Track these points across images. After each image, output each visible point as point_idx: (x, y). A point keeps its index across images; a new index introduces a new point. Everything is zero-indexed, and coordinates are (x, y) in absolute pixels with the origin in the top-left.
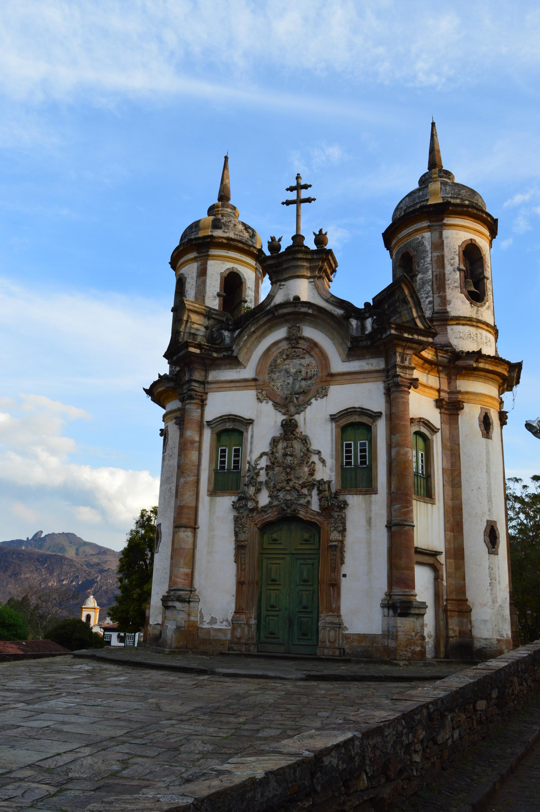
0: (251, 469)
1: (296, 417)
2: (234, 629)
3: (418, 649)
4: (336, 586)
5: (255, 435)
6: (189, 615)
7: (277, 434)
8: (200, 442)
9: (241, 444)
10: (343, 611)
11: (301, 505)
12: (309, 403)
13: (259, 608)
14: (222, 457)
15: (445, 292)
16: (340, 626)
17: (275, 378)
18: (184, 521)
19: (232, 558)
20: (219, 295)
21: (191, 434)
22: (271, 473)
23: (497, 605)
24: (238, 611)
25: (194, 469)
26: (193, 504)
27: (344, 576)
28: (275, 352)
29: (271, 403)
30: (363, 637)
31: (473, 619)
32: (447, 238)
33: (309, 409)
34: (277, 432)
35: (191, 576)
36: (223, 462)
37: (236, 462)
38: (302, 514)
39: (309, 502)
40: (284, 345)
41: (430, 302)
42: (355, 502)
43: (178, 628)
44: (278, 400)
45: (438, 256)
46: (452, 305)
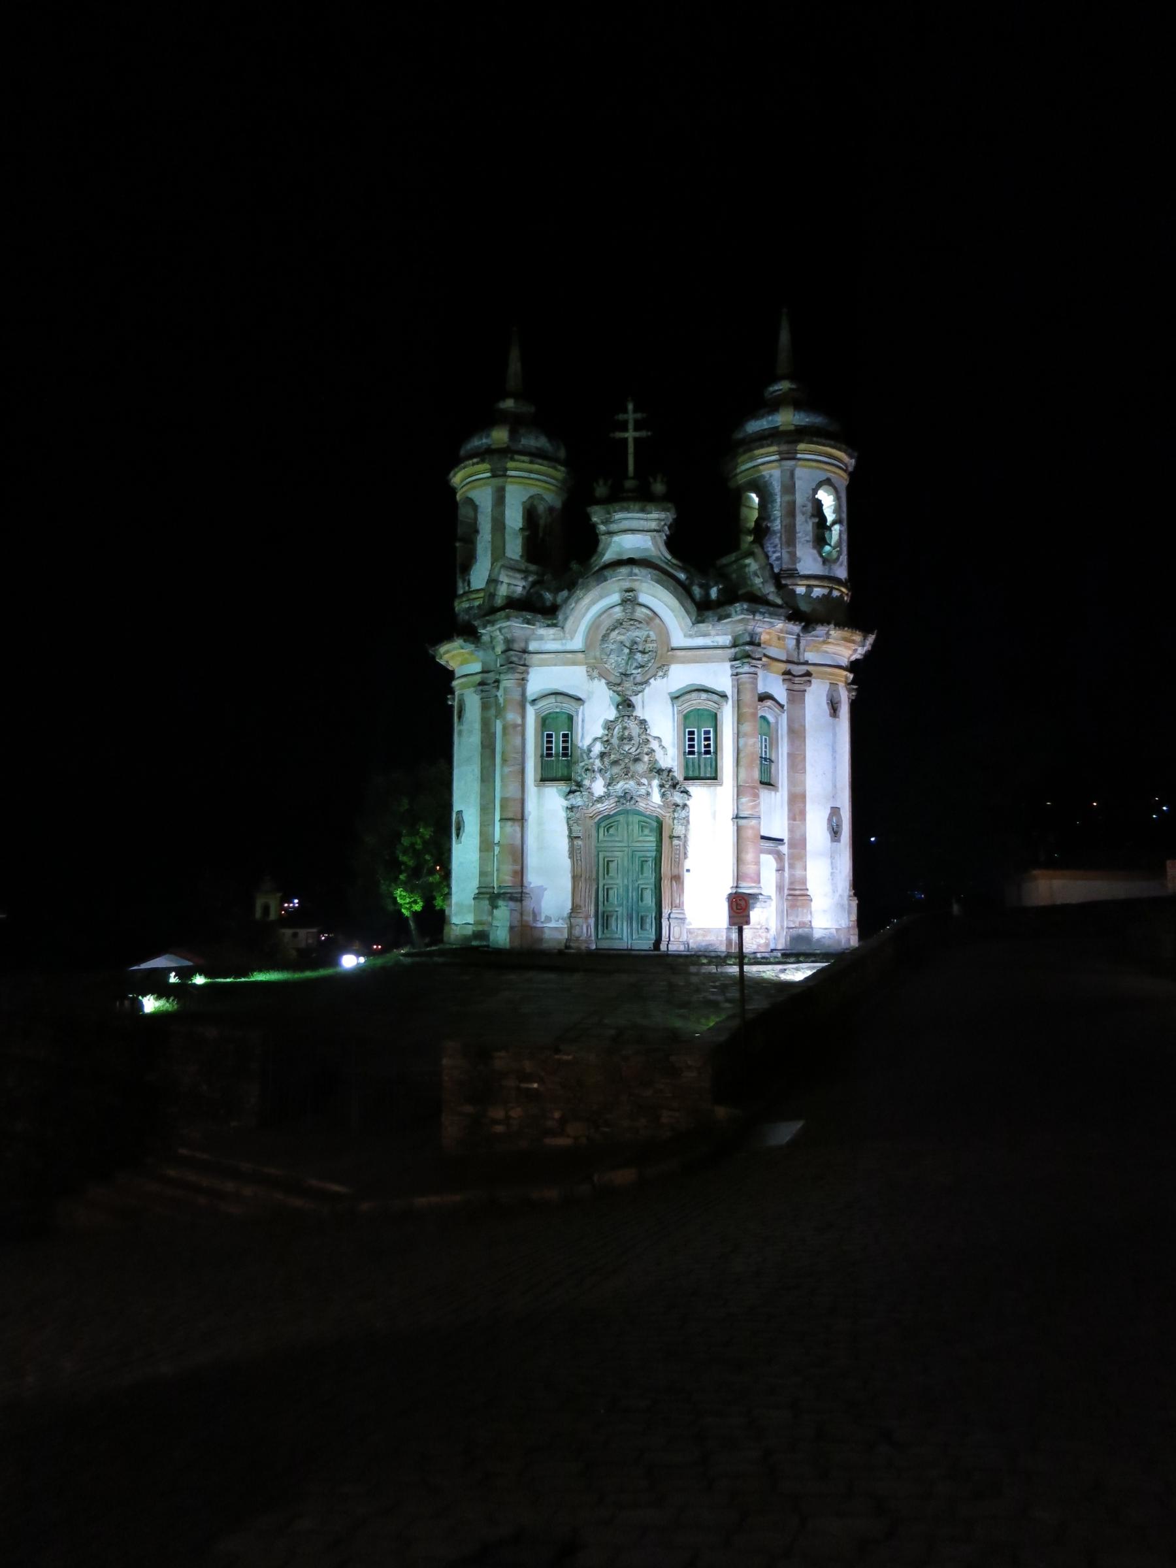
0: (585, 757)
1: (633, 699)
2: (571, 927)
3: (762, 941)
4: (677, 879)
5: (586, 719)
6: (522, 914)
7: (612, 718)
8: (523, 725)
9: (571, 728)
10: (686, 907)
11: (639, 796)
12: (646, 682)
13: (597, 905)
14: (548, 742)
15: (795, 546)
16: (683, 919)
17: (608, 651)
18: (510, 815)
19: (567, 854)
20: (522, 529)
21: (512, 716)
22: (606, 760)
23: (837, 895)
24: (575, 908)
25: (518, 756)
26: (519, 795)
27: (688, 871)
28: (607, 623)
29: (603, 681)
30: (707, 931)
31: (813, 909)
32: (800, 479)
33: (646, 691)
34: (612, 714)
35: (520, 873)
36: (549, 749)
37: (565, 748)
38: (642, 805)
39: (648, 794)
40: (618, 613)
41: (778, 559)
42: (699, 792)
43: (511, 928)
44: (612, 679)
45: (788, 502)
46: (802, 563)
